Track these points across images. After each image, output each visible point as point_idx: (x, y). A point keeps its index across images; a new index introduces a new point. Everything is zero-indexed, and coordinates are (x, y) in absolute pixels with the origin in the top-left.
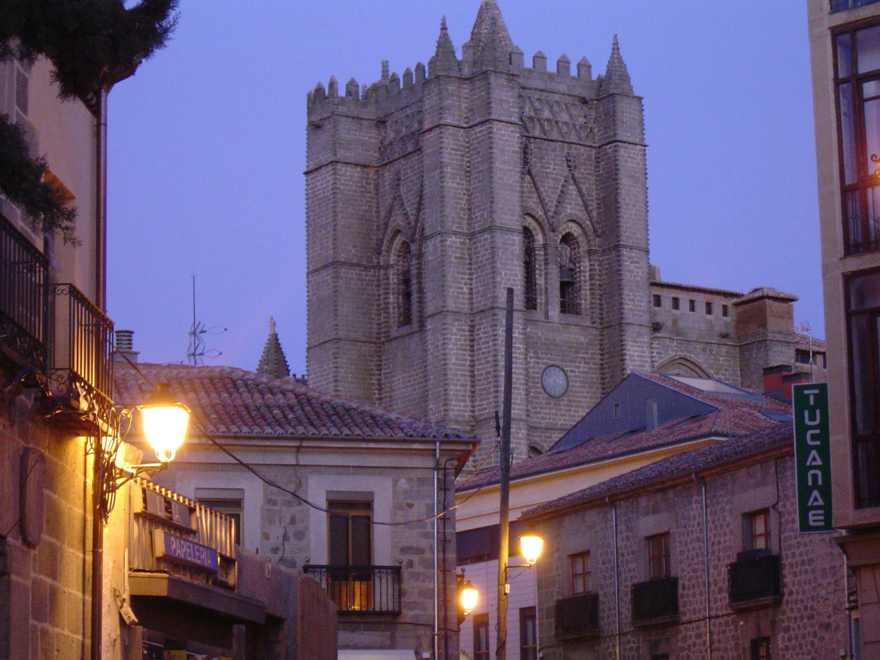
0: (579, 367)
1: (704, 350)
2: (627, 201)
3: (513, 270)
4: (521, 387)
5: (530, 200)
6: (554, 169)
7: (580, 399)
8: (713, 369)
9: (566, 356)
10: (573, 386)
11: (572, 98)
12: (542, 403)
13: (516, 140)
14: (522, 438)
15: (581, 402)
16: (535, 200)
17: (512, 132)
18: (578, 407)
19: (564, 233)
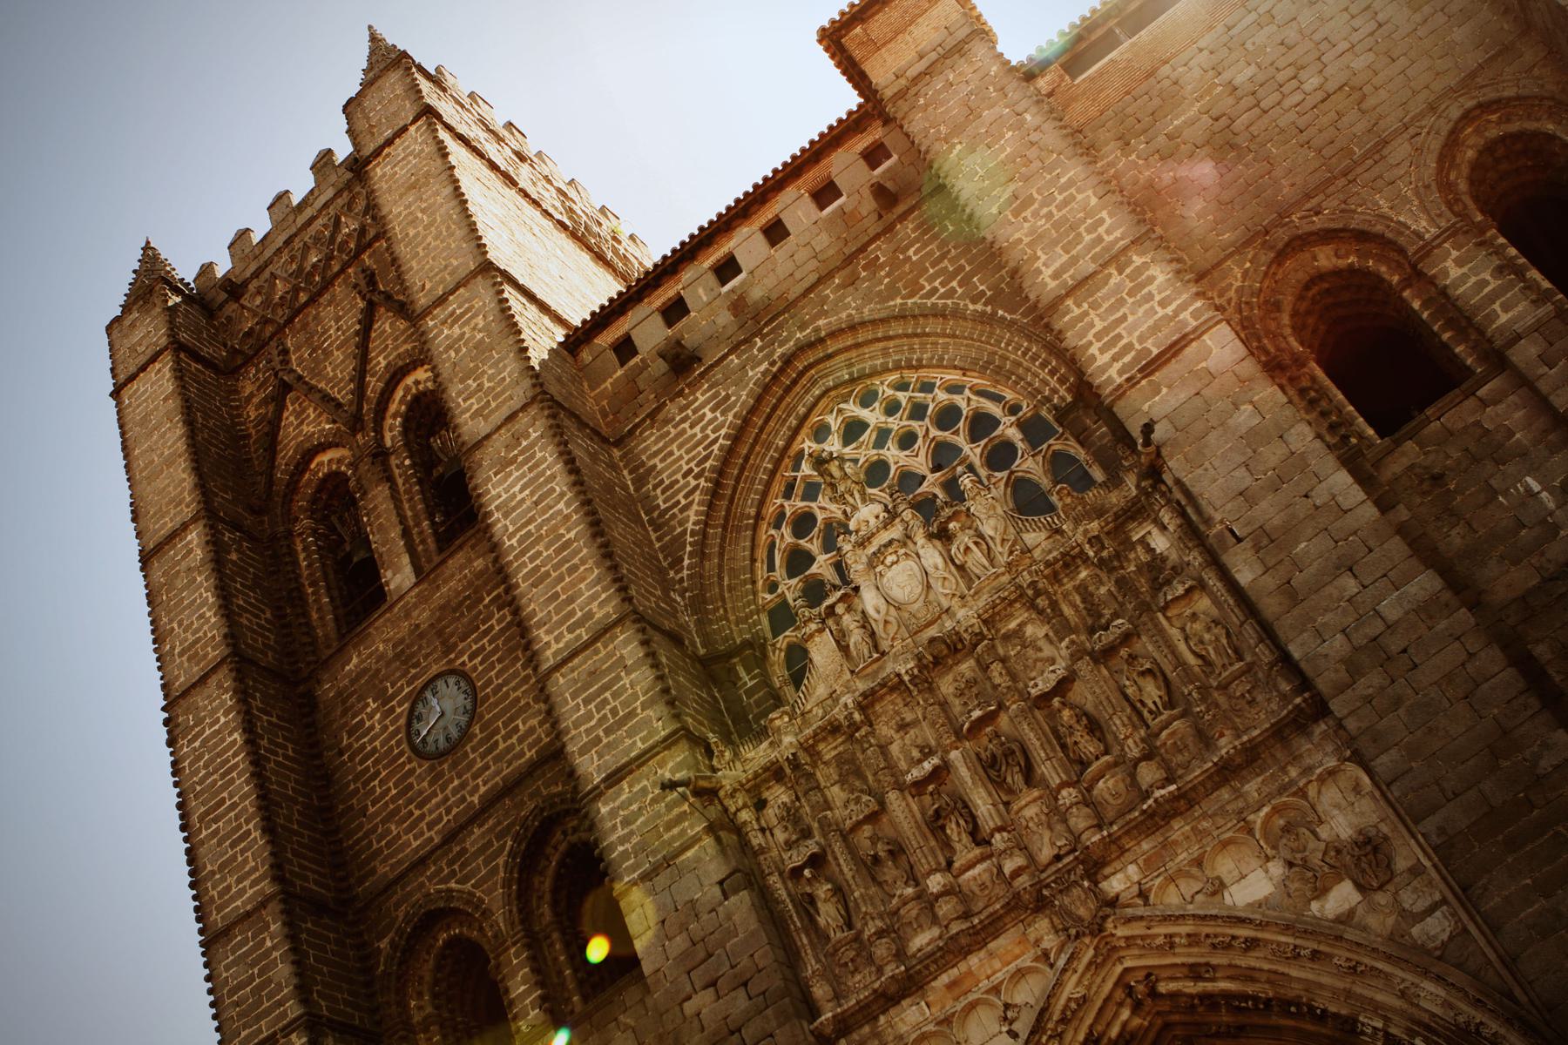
0: (486, 633)
1: (852, 281)
2: (412, 232)
3: (195, 600)
4: (251, 826)
5: (304, 427)
6: (338, 329)
7: (513, 695)
8: (896, 293)
9: (452, 635)
10: (490, 682)
11: (345, 194)
12: (421, 792)
13: (168, 375)
14: (274, 948)
15: (518, 700)
16: (312, 416)
17: (159, 370)
18: (512, 719)
19: (403, 407)
